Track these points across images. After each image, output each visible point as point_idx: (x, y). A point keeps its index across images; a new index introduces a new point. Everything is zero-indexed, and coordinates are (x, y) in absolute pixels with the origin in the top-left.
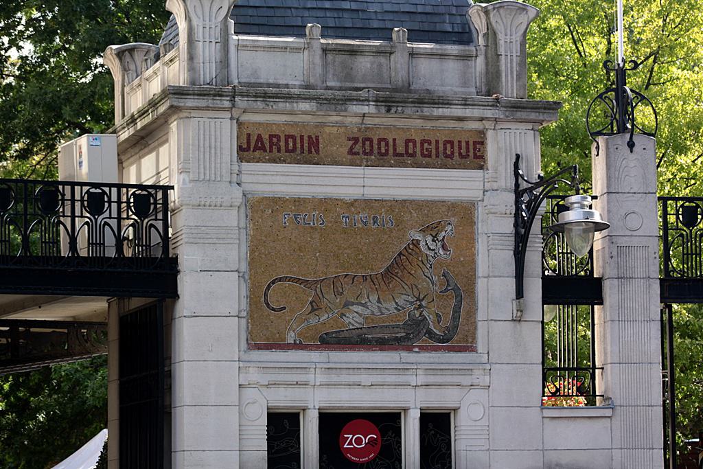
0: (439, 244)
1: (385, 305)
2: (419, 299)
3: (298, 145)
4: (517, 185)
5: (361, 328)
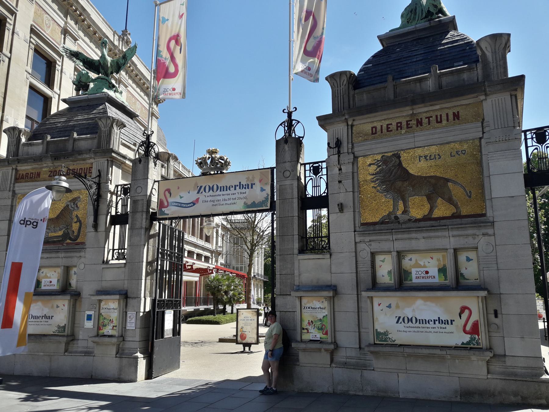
2: (67, 226)
3: (34, 176)
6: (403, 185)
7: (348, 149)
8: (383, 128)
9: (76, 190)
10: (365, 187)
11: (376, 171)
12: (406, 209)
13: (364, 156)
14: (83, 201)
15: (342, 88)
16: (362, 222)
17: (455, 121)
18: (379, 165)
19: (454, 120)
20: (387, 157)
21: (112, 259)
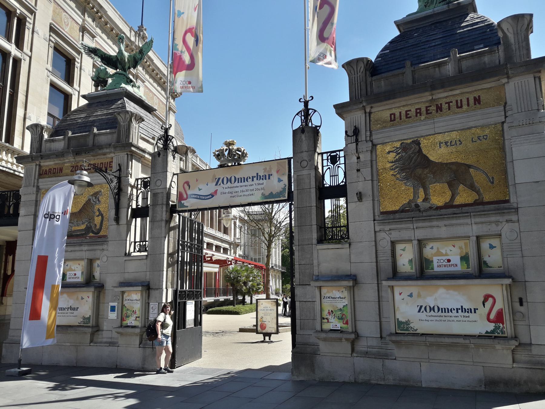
1: (79, 223)
3: (56, 171)
6: (423, 172)
7: (366, 137)
8: (402, 115)
9: (97, 184)
10: (384, 175)
11: (395, 159)
12: (427, 197)
13: (383, 144)
14: (105, 195)
15: (359, 76)
16: (381, 211)
17: (476, 106)
18: (398, 152)
19: (475, 104)
20: (407, 144)
21: (134, 252)
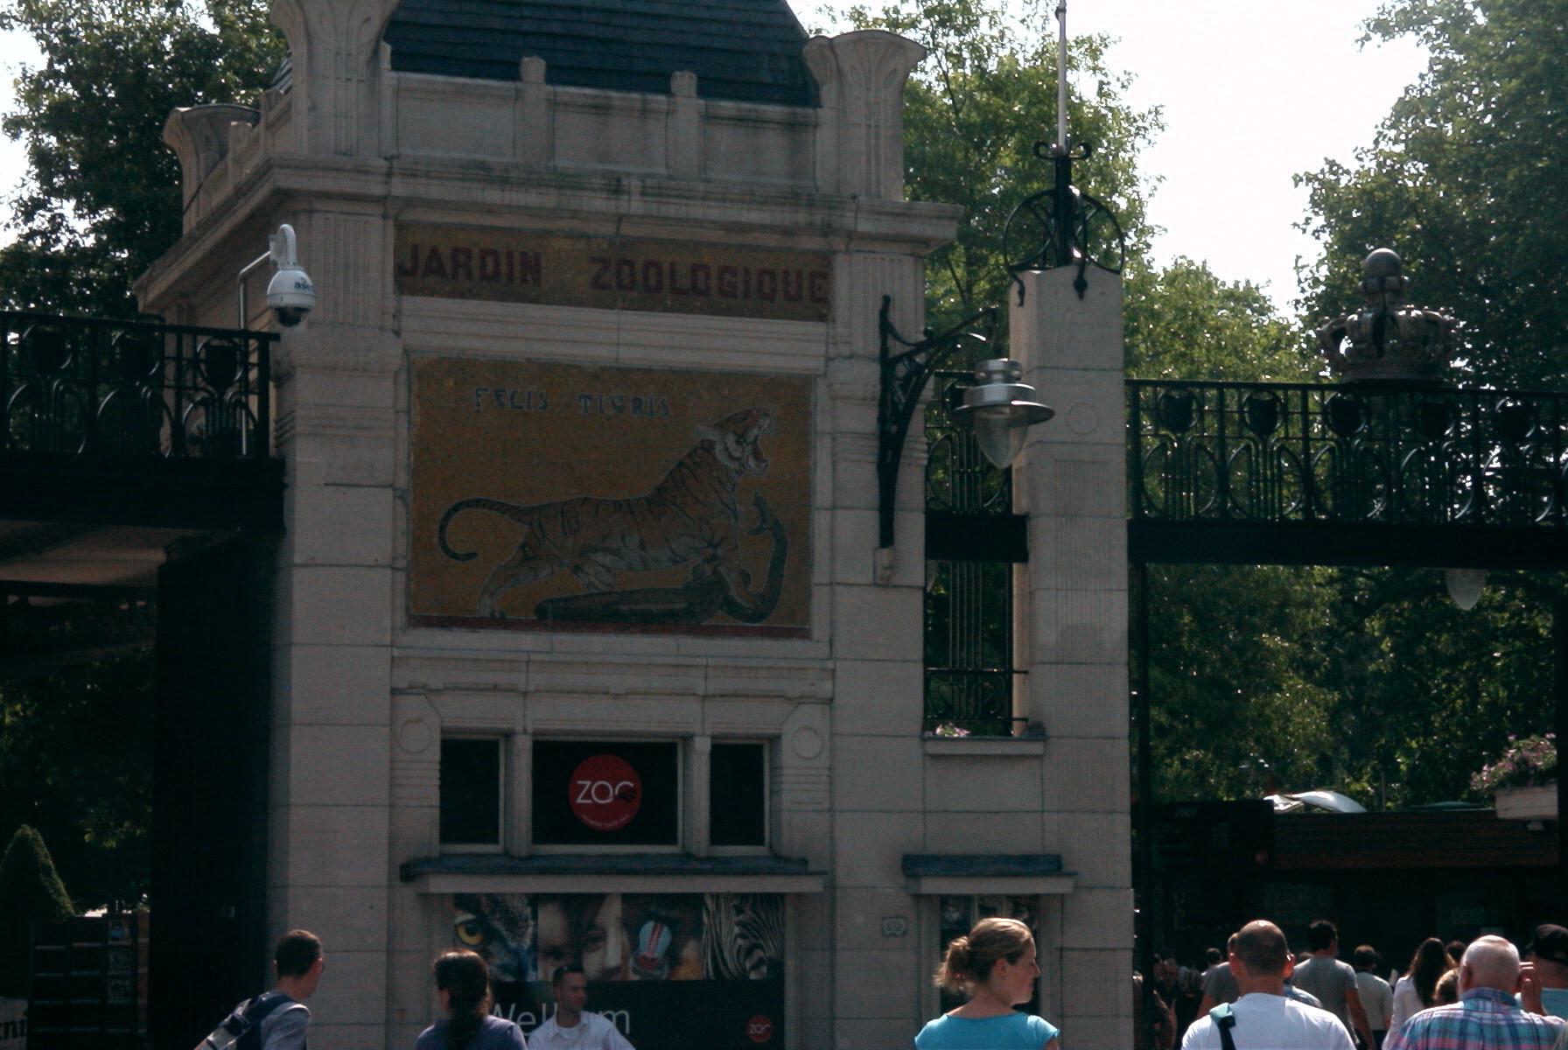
0: (749, 449)
2: (710, 545)
3: (504, 268)
4: (884, 350)
5: (610, 593)
